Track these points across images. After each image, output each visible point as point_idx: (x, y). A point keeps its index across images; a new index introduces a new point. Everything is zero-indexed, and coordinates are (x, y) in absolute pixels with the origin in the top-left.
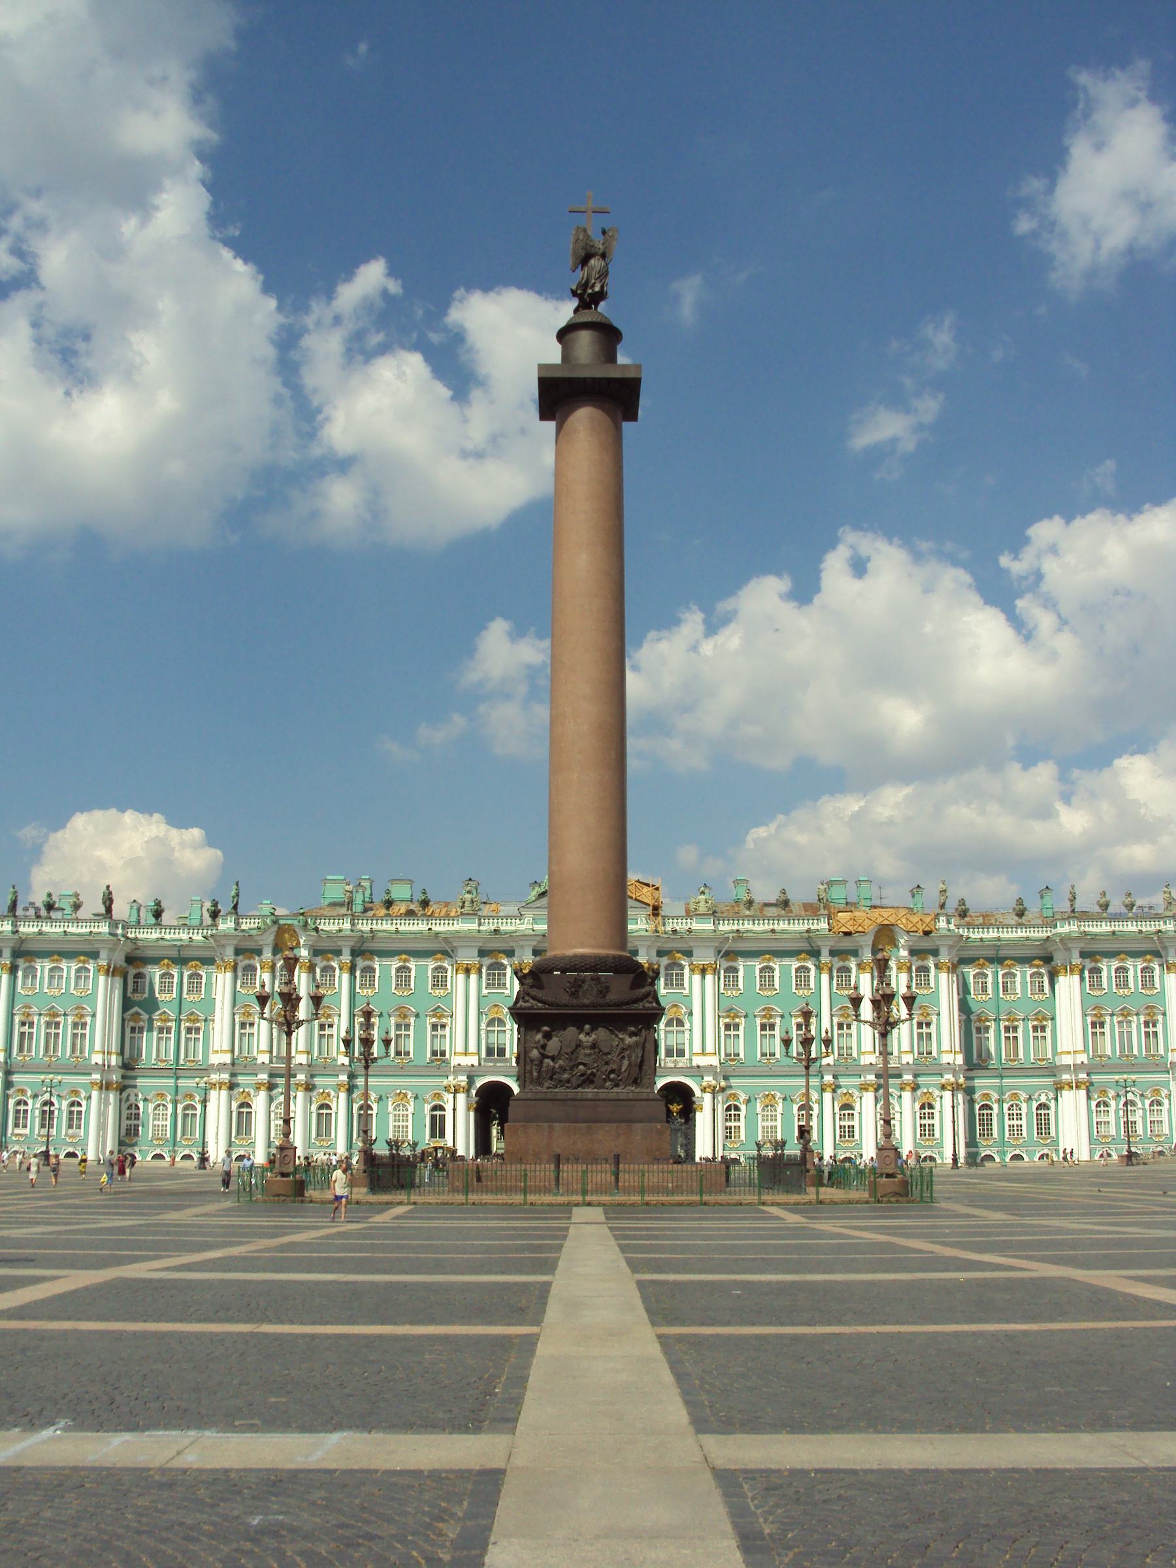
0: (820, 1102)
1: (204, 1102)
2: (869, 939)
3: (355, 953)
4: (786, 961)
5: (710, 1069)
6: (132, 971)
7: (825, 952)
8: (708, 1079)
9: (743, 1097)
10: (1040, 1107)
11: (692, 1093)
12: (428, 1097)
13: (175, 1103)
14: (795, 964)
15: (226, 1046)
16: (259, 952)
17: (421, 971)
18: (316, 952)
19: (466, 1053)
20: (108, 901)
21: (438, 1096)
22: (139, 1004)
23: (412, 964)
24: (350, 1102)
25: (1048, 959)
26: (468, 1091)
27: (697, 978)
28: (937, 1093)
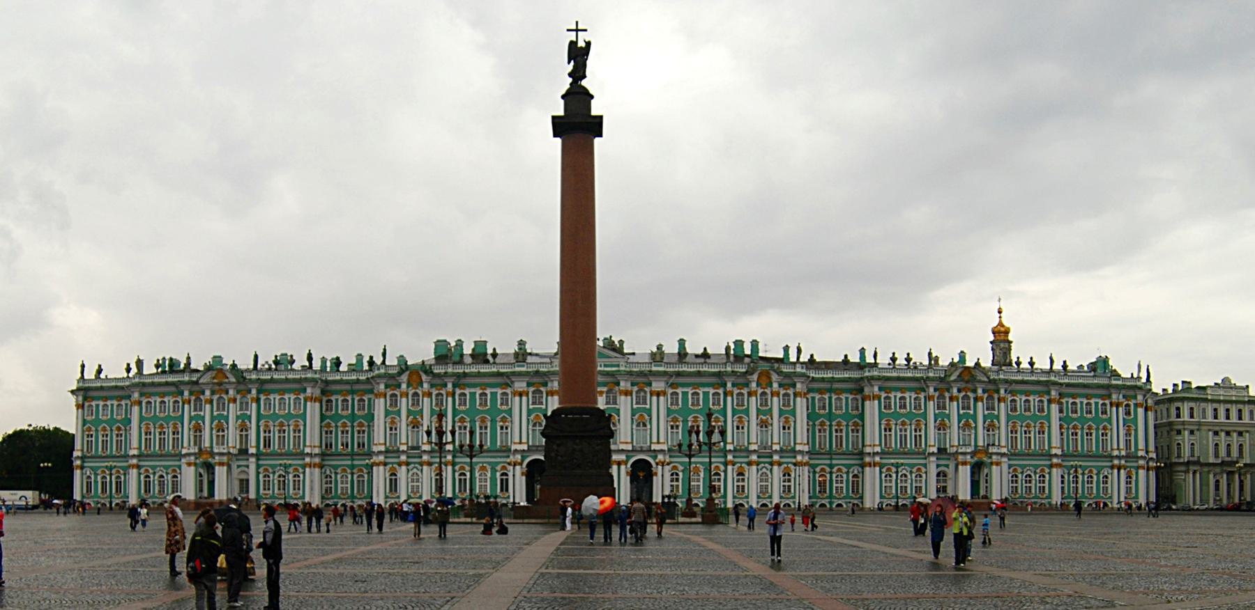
0: (725, 471)
1: (370, 473)
2: (755, 377)
3: (454, 386)
4: (706, 390)
5: (662, 451)
6: (325, 399)
7: (729, 385)
8: (660, 457)
9: (681, 468)
10: (855, 476)
11: (651, 465)
12: (498, 468)
13: (352, 474)
14: (712, 391)
15: (382, 441)
16: (399, 386)
17: (494, 395)
18: (432, 386)
19: (521, 443)
20: (310, 358)
21: (504, 468)
22: (329, 417)
23: (488, 391)
24: (454, 471)
25: (861, 390)
26: (521, 464)
27: (655, 398)
28: (792, 467)
